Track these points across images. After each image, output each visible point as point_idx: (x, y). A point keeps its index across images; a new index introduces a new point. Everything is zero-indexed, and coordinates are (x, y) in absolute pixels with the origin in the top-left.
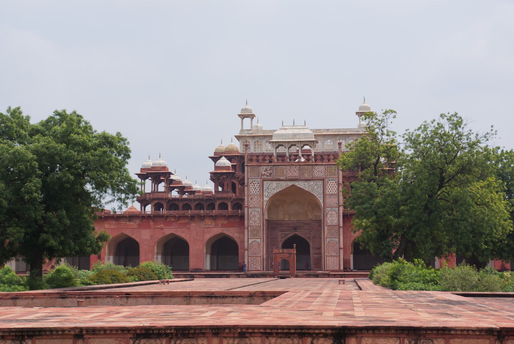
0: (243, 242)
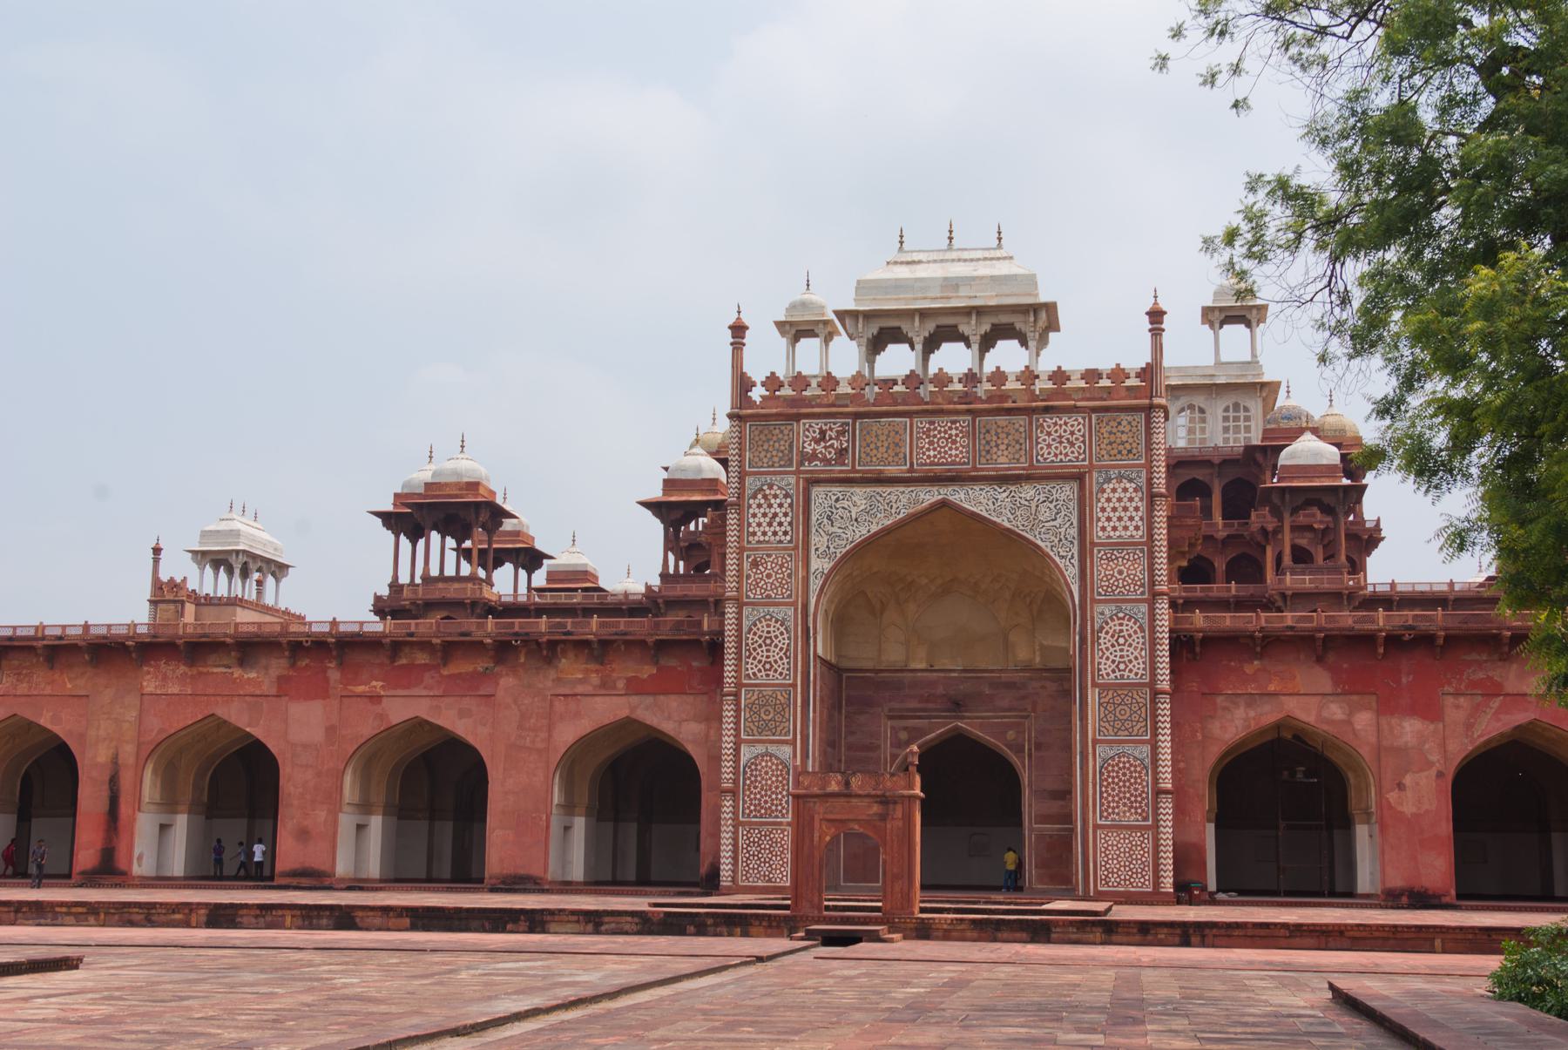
0: (716, 759)
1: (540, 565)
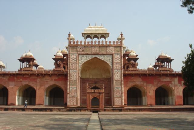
1: (38, 67)
